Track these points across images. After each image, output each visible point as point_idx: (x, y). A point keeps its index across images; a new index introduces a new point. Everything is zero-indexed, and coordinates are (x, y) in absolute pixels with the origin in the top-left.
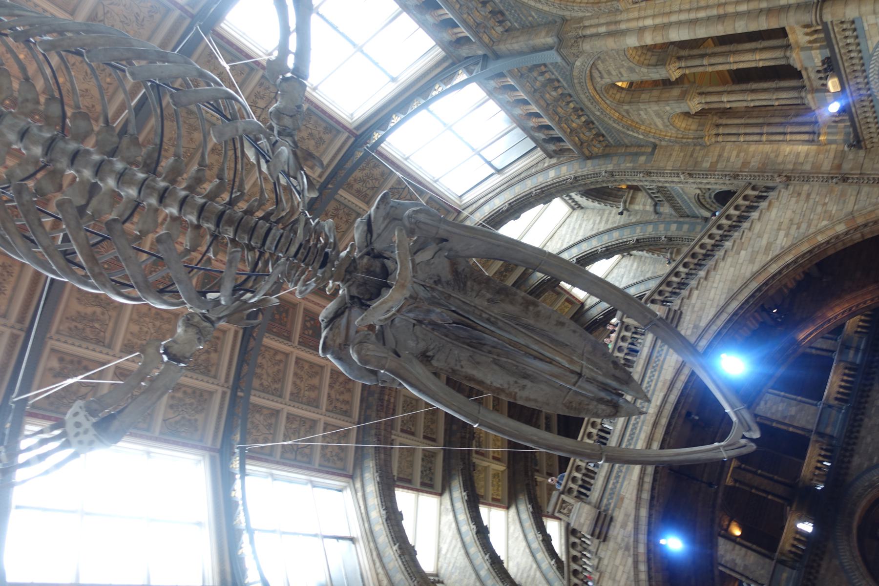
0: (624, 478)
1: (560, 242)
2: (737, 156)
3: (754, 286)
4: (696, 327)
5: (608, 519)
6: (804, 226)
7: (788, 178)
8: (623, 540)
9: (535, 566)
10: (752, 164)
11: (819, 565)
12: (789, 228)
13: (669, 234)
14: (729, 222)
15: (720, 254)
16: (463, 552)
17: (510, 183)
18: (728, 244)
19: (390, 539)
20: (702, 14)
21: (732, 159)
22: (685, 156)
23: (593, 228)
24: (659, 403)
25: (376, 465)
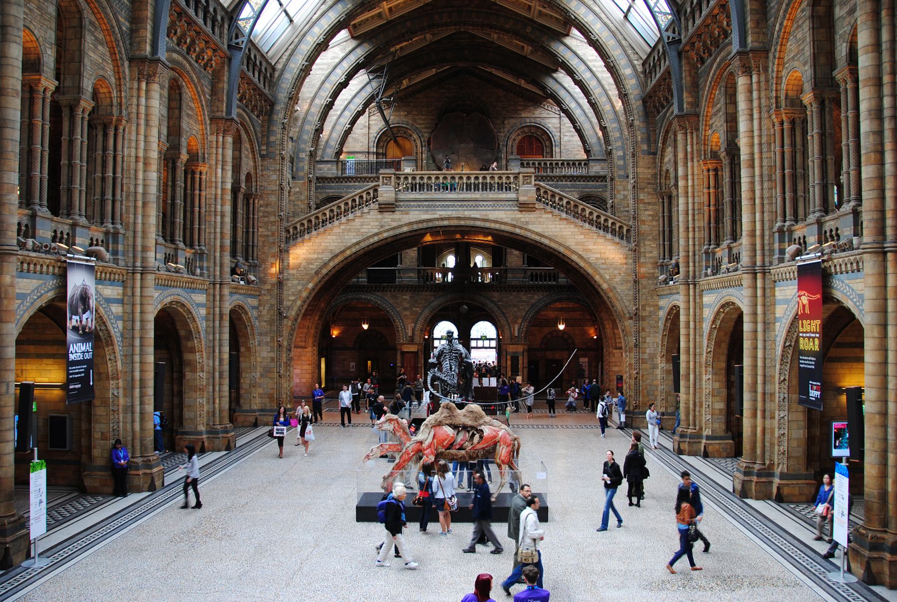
0: (420, 210)
2: (649, 215)
3: (561, 249)
4: (527, 223)
6: (605, 266)
7: (635, 251)
8: (385, 222)
9: (339, 113)
10: (644, 227)
11: (426, 291)
13: (614, 151)
14: (602, 222)
16: (323, 78)
17: (617, 32)
18: (587, 225)
19: (308, 55)
20: (690, 218)
21: (647, 213)
22: (648, 179)
24: (472, 216)
25: (351, 11)
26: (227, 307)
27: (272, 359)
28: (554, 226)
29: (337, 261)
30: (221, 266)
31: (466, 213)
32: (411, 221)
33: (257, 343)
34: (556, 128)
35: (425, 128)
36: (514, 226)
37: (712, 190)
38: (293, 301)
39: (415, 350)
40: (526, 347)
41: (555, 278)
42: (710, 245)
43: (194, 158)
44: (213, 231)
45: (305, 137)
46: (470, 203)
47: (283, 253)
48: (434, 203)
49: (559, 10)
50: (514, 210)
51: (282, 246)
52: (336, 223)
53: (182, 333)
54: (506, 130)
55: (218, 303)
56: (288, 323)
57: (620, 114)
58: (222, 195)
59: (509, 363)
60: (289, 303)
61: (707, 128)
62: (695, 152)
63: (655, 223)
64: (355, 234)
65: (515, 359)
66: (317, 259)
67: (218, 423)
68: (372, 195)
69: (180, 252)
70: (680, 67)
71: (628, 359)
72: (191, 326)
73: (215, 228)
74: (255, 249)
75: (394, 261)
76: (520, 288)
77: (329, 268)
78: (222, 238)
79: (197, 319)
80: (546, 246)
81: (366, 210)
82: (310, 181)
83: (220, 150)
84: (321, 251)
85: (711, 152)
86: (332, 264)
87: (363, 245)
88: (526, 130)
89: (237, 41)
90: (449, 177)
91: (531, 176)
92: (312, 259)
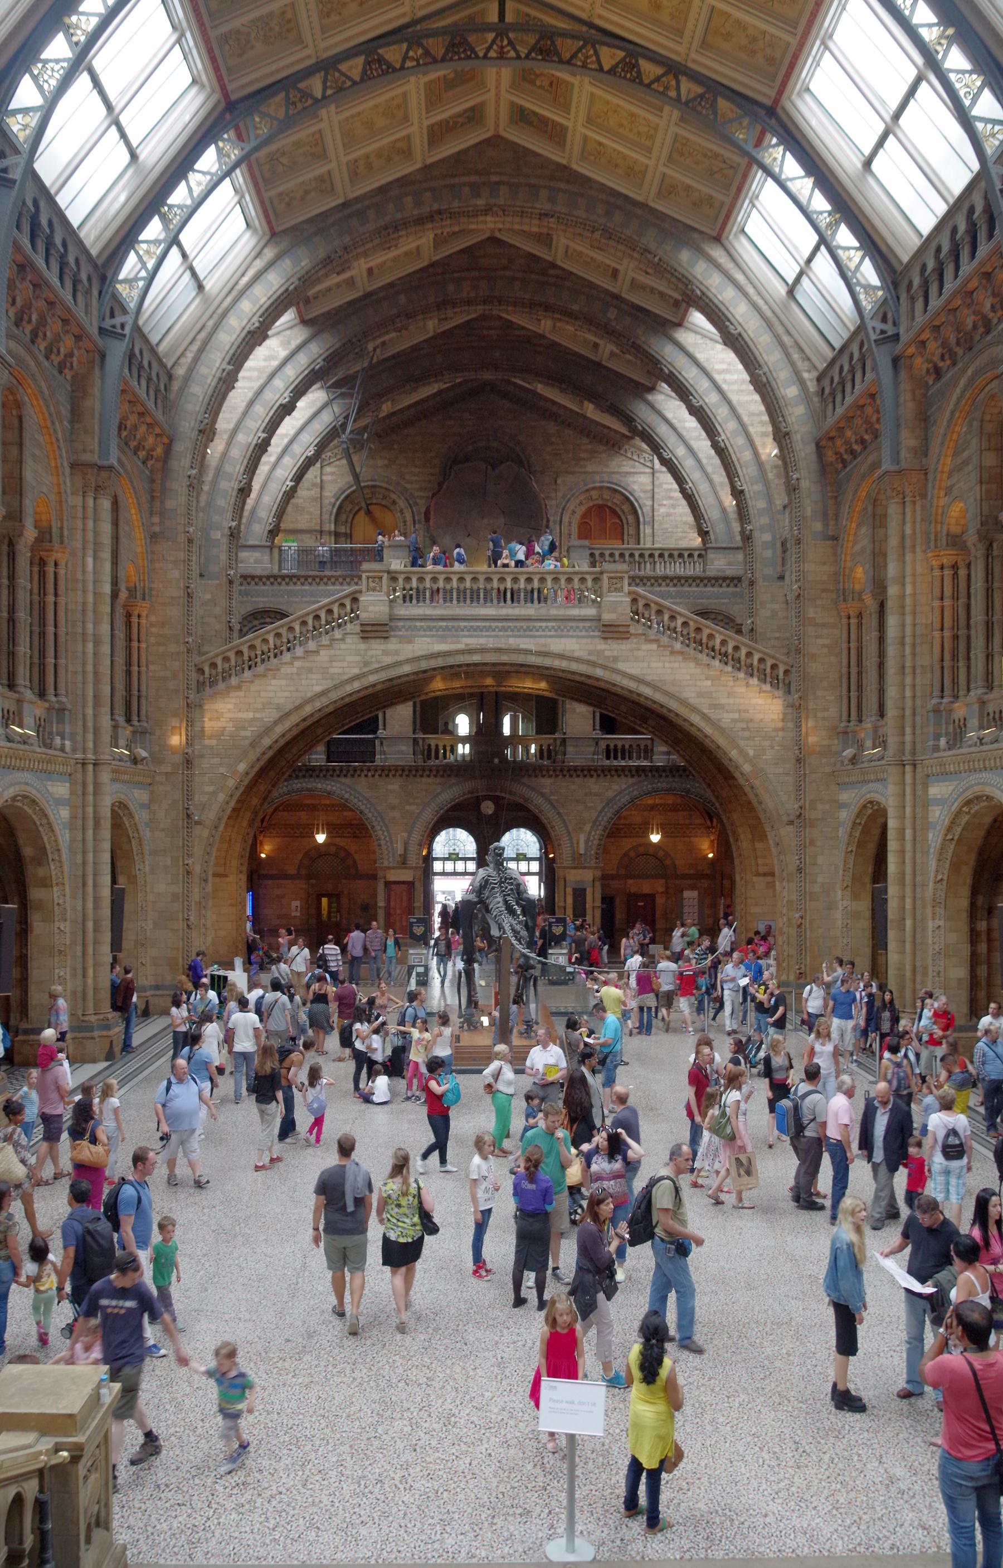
0: (433, 636)
1: (724, 366)
2: (824, 646)
3: (673, 705)
4: (616, 659)
5: (385, 635)
6: (746, 734)
12: (742, 721)
13: (756, 534)
15: (703, 658)
17: (774, 320)
19: (232, 352)
20: (908, 650)
21: (820, 641)
23: (753, 414)
24: (522, 646)
26: (107, 802)
27: (175, 897)
28: (660, 665)
29: (288, 724)
30: (96, 731)
31: (513, 642)
32: (417, 654)
33: (147, 869)
34: (645, 492)
35: (421, 489)
36: (594, 664)
37: (947, 602)
38: (213, 794)
39: (411, 879)
40: (598, 873)
41: (647, 752)
42: (942, 697)
43: (44, 536)
44: (80, 669)
45: (221, 502)
46: (519, 624)
47: (192, 710)
48: (455, 624)
49: (673, 280)
50: (594, 637)
51: (192, 696)
52: (287, 657)
53: (28, 852)
54: (560, 494)
55: (90, 798)
56: (202, 833)
57: (768, 468)
58: (95, 604)
59: (570, 900)
60: (204, 798)
61: (942, 493)
62: (918, 536)
63: (833, 659)
64: (319, 676)
65: (579, 894)
66: (254, 719)
67: (92, 1012)
68: (348, 607)
69: (26, 707)
70: (896, 384)
71: (785, 893)
72: (45, 839)
73: (84, 664)
74: (143, 701)
75: (371, 725)
76: (587, 771)
77: (274, 736)
78: (97, 682)
79: (56, 827)
80: (646, 698)
81: (337, 634)
82: (231, 582)
83: (90, 524)
84: (260, 706)
85: (948, 535)
86: (279, 730)
87: (334, 696)
88: (594, 494)
89: (113, 322)
90: (482, 578)
91: (622, 578)
92: (245, 720)
